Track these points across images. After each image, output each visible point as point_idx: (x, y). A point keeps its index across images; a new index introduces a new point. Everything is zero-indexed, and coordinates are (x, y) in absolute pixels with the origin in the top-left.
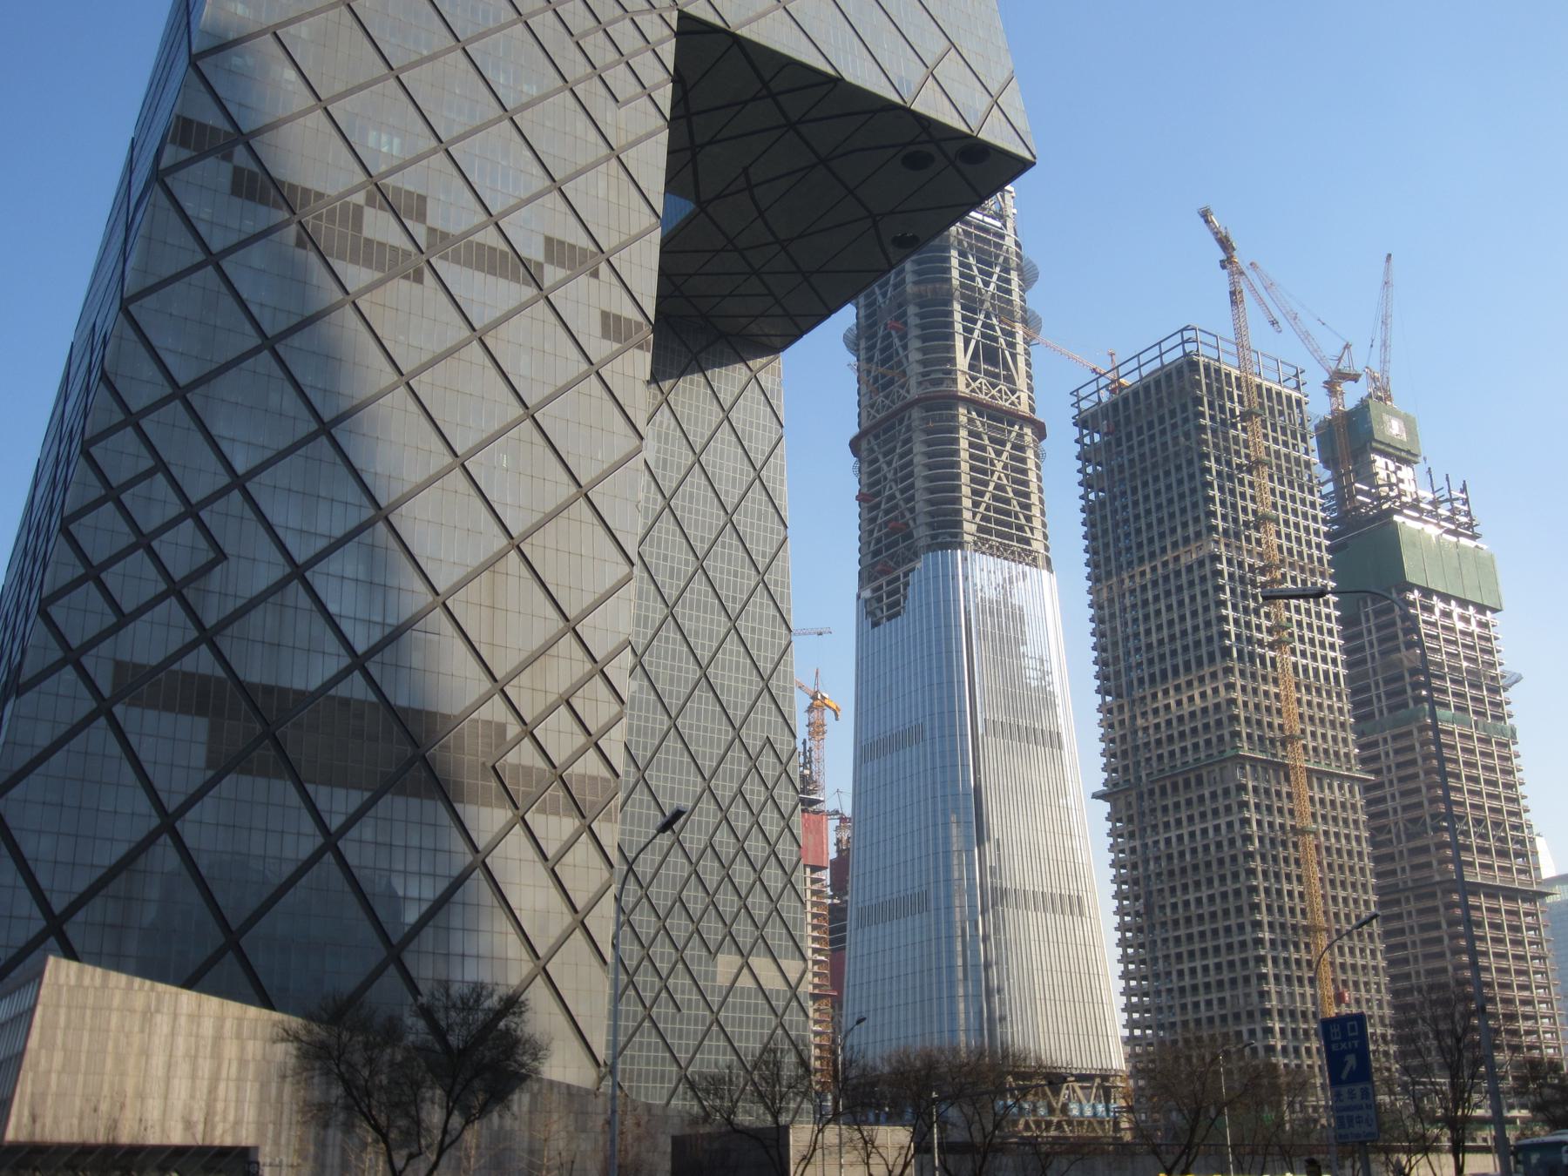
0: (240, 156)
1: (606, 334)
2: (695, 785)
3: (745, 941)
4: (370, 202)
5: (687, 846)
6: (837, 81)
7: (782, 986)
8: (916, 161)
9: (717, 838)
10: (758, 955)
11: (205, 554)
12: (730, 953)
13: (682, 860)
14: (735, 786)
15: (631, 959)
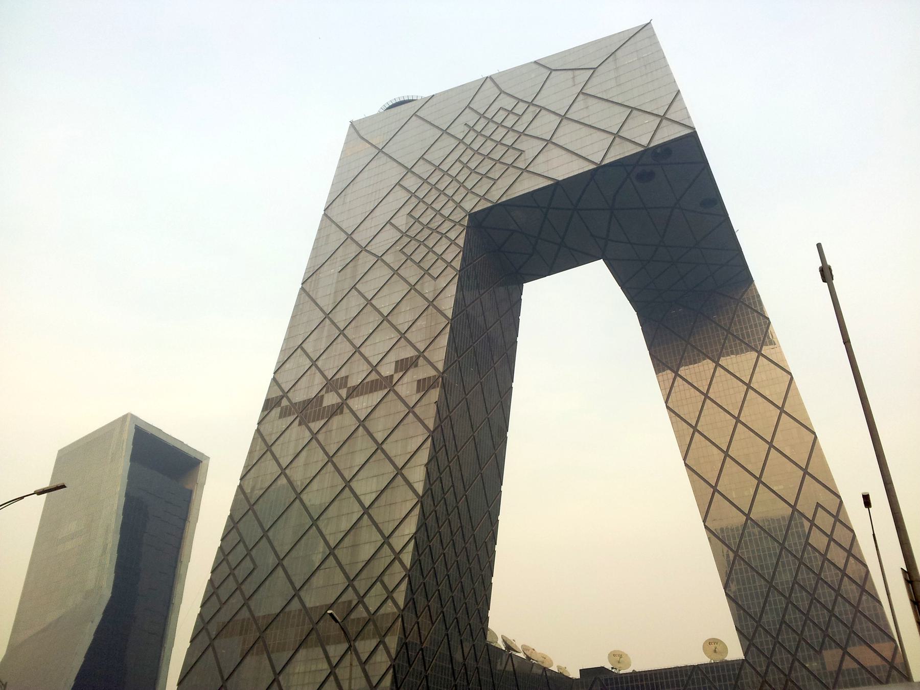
0: (285, 402)
1: (418, 391)
2: (774, 548)
3: (841, 637)
4: (327, 392)
5: (780, 588)
6: (557, 184)
7: (878, 661)
8: (646, 177)
9: (800, 577)
10: (854, 645)
11: (252, 567)
12: (831, 648)
13: (778, 598)
14: (803, 541)
15: (761, 666)
